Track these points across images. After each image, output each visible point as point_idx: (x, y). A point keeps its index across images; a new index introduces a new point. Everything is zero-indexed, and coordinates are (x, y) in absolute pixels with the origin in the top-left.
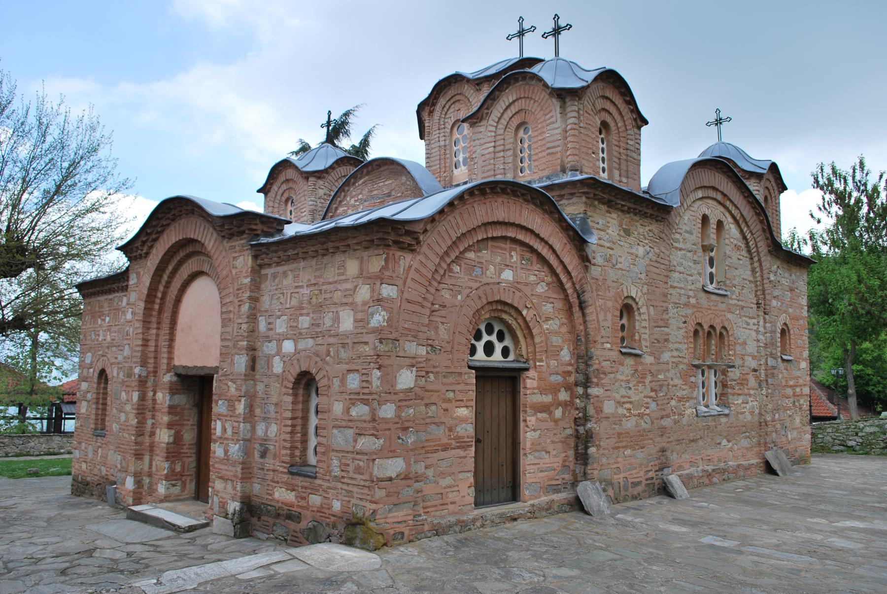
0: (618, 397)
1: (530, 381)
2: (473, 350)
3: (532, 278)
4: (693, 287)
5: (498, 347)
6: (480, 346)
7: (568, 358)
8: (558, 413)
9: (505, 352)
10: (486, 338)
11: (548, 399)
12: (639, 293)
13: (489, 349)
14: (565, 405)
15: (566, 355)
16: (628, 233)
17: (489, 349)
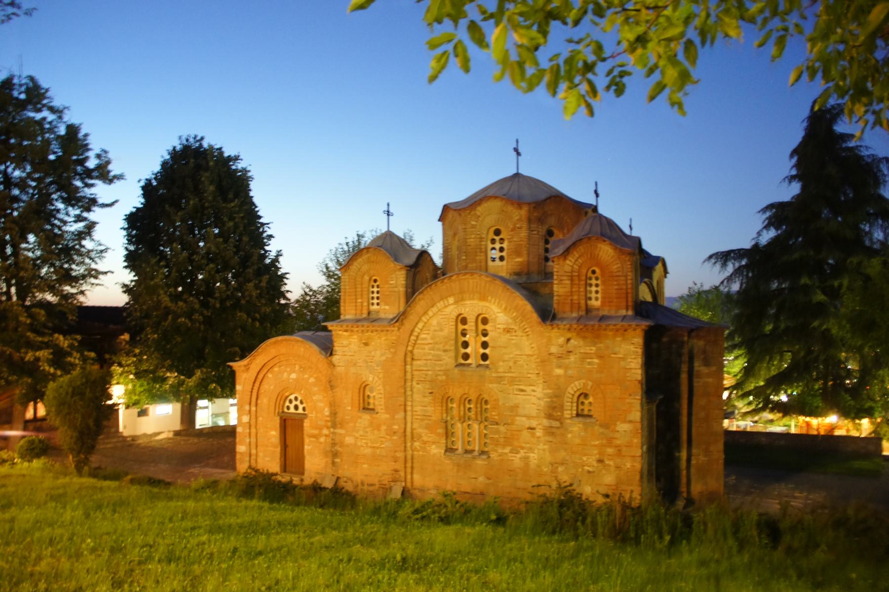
0: (357, 435)
1: (306, 423)
2: (288, 408)
3: (306, 376)
4: (443, 368)
5: (301, 407)
6: (292, 406)
7: (327, 413)
8: (322, 439)
9: (304, 409)
10: (294, 403)
11: (316, 432)
12: (376, 379)
13: (296, 407)
14: (326, 436)
15: (327, 412)
16: (366, 344)
17: (296, 407)
